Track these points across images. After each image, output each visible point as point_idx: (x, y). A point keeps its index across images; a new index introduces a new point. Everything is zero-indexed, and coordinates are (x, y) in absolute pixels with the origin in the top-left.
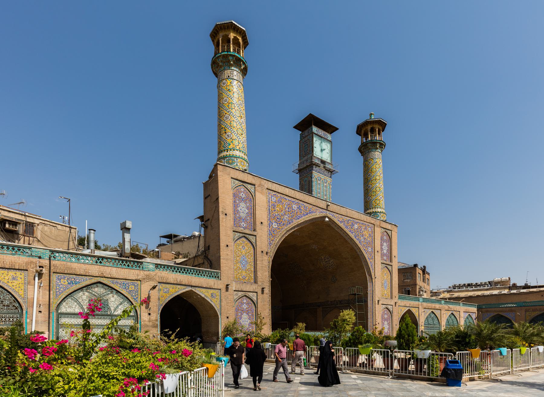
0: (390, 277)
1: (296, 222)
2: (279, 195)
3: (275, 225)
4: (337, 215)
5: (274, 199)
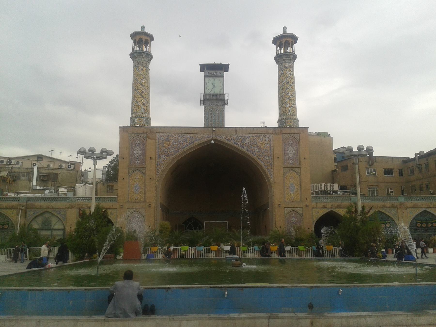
0: (298, 179)
1: (181, 151)
2: (167, 135)
3: (163, 157)
4: (225, 136)
5: (162, 139)
